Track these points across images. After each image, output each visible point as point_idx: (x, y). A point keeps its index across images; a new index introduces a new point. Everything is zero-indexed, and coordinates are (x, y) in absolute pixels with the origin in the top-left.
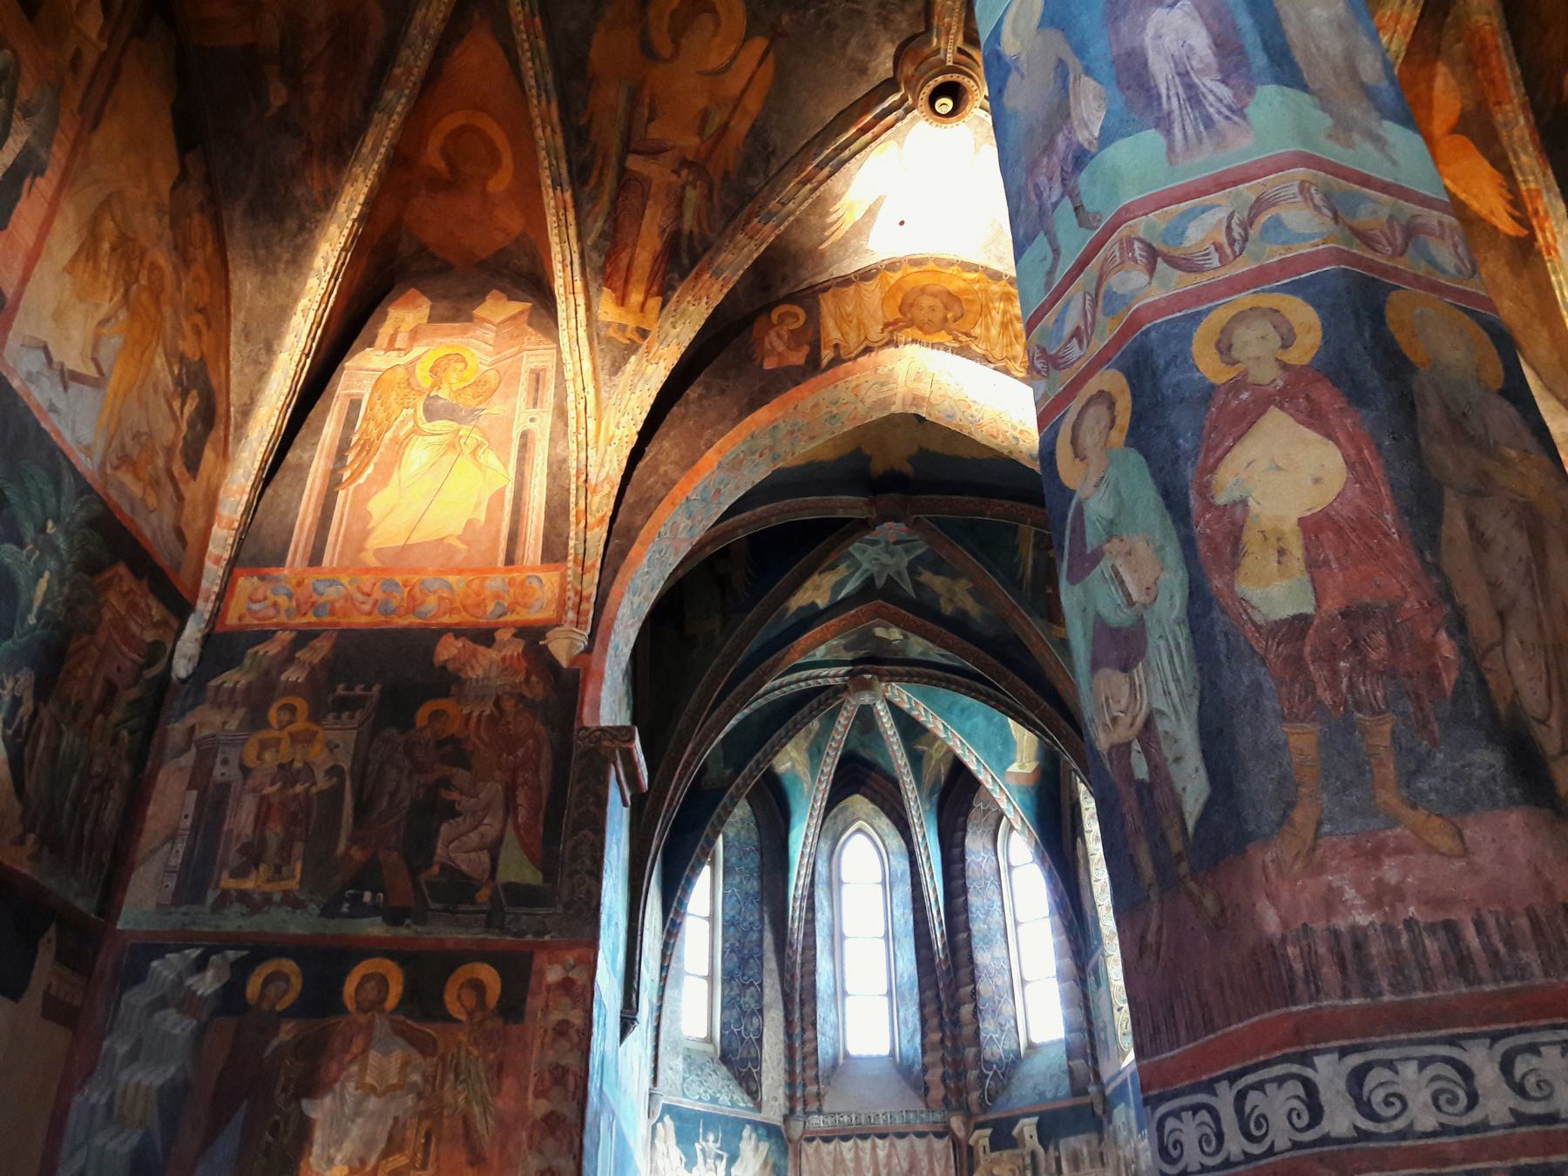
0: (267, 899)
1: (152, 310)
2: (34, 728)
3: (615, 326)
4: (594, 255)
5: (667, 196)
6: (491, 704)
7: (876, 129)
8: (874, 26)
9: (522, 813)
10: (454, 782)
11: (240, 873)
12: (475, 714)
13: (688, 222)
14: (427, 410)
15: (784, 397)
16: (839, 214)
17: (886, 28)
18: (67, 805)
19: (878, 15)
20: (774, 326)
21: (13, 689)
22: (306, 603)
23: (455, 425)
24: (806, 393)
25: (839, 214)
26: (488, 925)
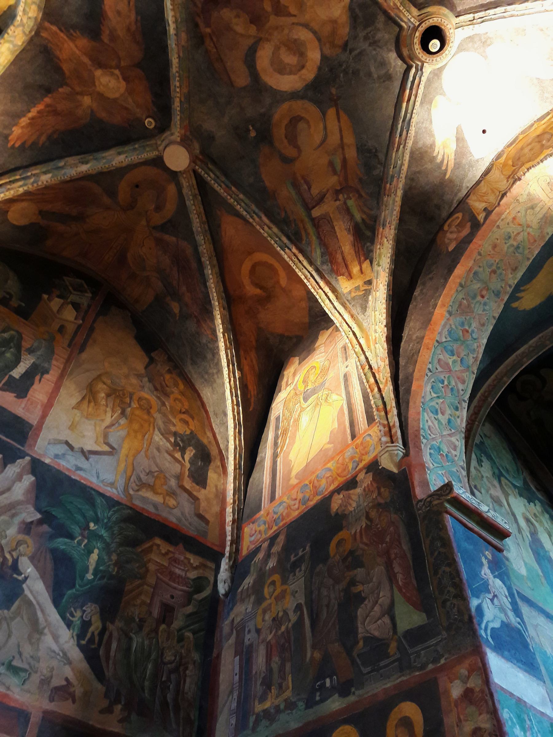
0: (278, 710)
1: (146, 417)
2: (106, 637)
3: (354, 290)
4: (325, 267)
5: (340, 213)
6: (364, 519)
7: (414, 92)
8: (374, 52)
9: (400, 577)
10: (358, 580)
11: (263, 699)
12: (358, 531)
13: (358, 216)
14: (304, 399)
15: (467, 253)
16: (441, 153)
17: (380, 47)
18: (147, 683)
19: (370, 45)
20: (447, 231)
21: (82, 617)
22: (271, 521)
23: (316, 395)
24: (480, 243)
25: (441, 153)
26: (401, 669)
